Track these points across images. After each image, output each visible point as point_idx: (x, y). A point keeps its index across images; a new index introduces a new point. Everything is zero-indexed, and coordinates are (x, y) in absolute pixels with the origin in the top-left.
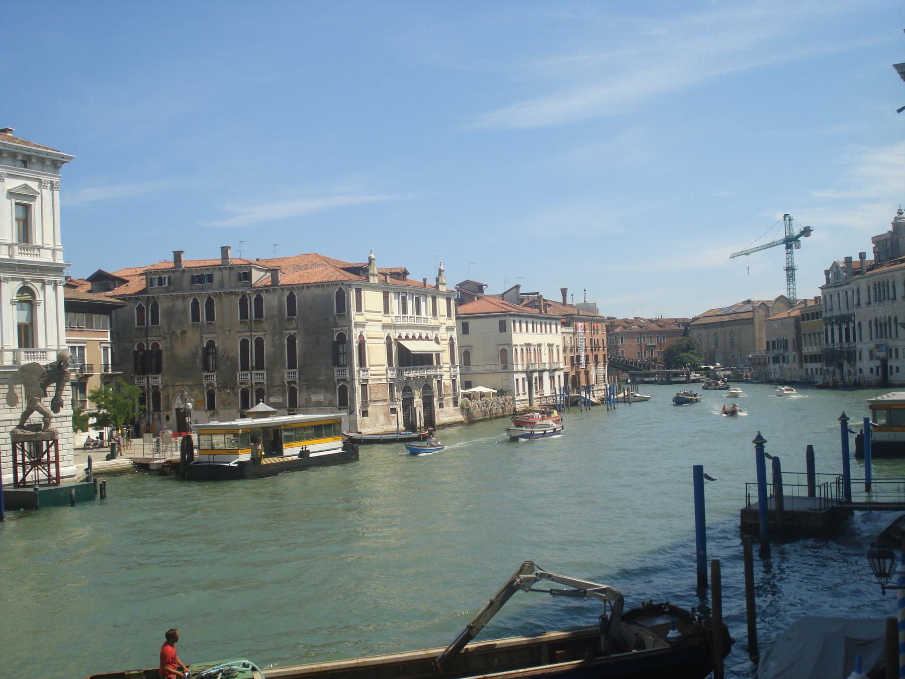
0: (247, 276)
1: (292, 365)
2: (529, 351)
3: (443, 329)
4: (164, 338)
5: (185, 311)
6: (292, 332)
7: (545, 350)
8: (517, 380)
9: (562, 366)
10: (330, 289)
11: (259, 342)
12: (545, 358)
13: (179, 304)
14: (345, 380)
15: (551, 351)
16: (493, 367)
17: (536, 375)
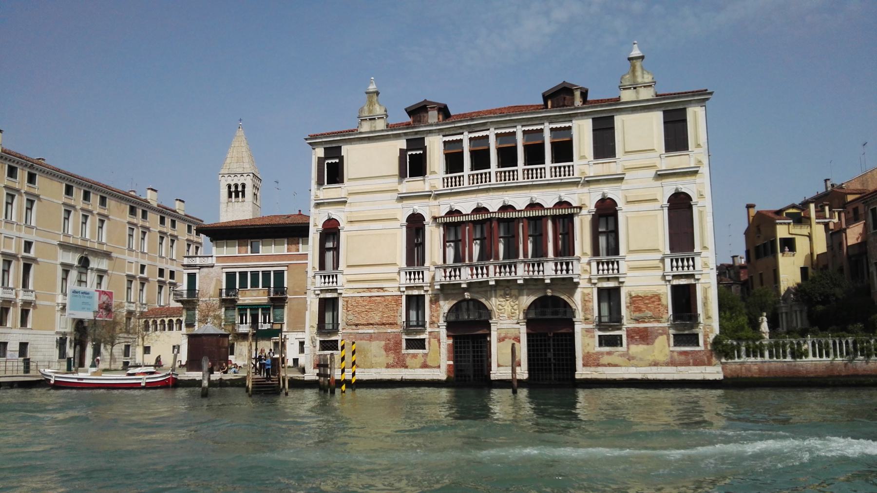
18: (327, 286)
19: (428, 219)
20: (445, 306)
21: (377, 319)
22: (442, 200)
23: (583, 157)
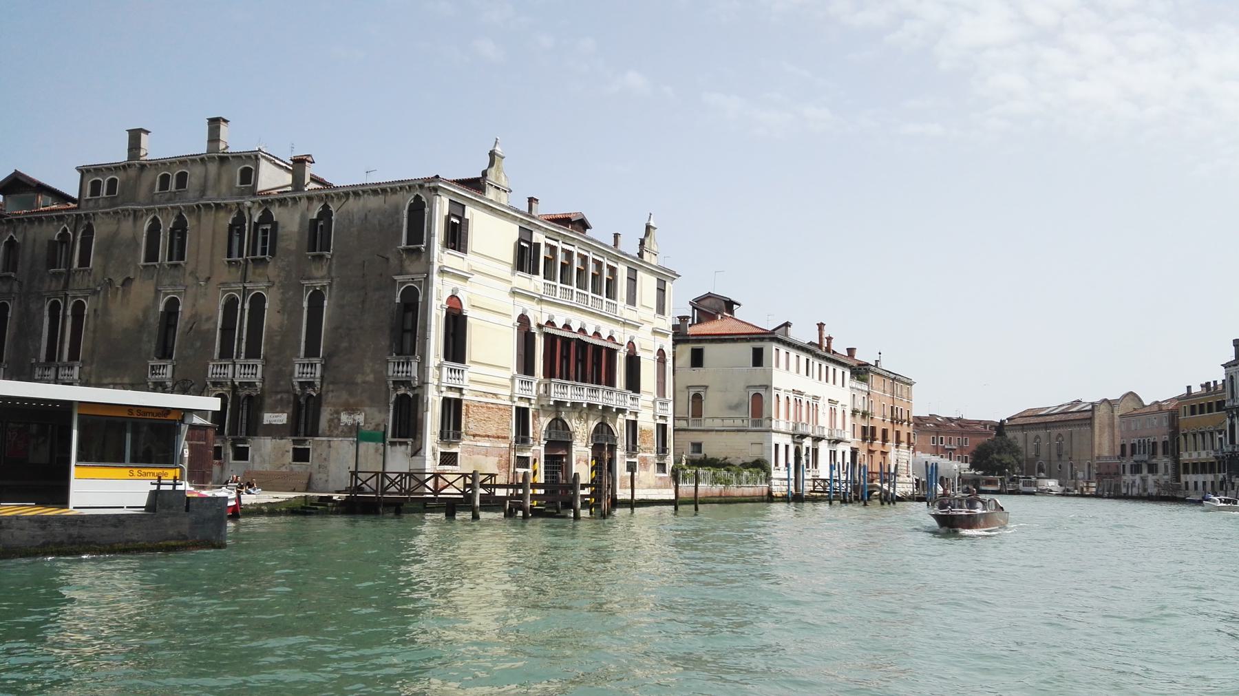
0: (248, 176)
1: (312, 351)
2: (798, 403)
3: (646, 330)
4: (95, 292)
5: (135, 242)
6: (318, 284)
7: (824, 408)
8: (777, 446)
9: (848, 437)
10: (397, 198)
11: (258, 301)
12: (824, 420)
13: (127, 227)
14: (407, 383)
15: (833, 412)
16: (738, 423)
17: (808, 442)
18: (453, 383)
19: (533, 326)
20: (544, 422)
21: (493, 432)
22: (545, 307)
23: (622, 300)
